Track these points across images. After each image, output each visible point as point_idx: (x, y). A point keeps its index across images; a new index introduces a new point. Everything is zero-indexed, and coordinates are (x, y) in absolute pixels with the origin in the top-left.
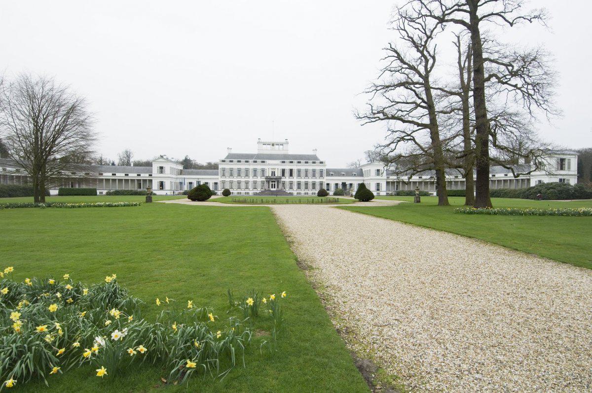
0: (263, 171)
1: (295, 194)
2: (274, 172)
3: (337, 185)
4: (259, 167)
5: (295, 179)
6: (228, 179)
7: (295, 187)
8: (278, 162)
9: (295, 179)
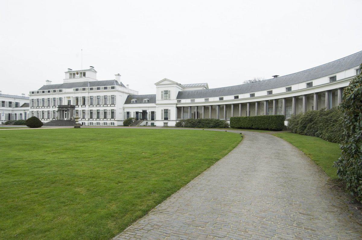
0: (60, 99)
1: (87, 125)
2: (70, 100)
3: (137, 113)
4: (57, 96)
5: (87, 108)
6: (35, 110)
7: (87, 116)
8: (71, 90)
9: (87, 108)
